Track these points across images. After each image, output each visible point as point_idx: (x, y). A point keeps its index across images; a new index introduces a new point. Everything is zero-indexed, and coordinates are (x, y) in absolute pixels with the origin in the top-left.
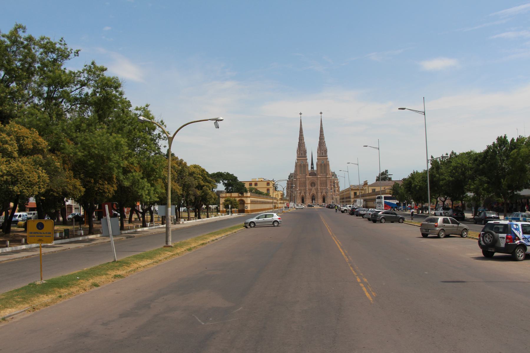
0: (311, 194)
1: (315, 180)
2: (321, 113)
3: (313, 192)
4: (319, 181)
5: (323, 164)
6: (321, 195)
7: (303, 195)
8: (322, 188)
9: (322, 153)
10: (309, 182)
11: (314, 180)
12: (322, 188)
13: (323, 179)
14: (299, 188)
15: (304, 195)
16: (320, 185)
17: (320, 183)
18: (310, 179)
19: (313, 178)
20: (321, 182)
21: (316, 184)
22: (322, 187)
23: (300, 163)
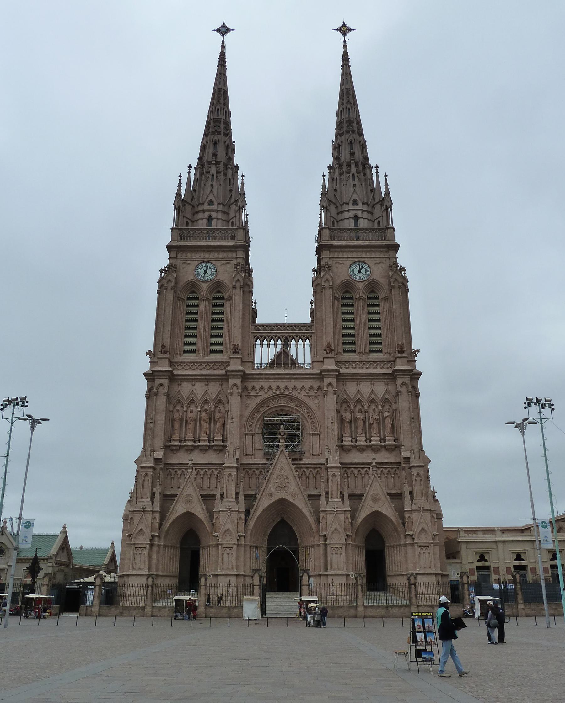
0: (263, 504)
1: (301, 396)
2: (344, 30)
3: (283, 487)
4: (330, 403)
5: (361, 286)
6: (353, 517)
7: (189, 515)
8: (355, 457)
9: (356, 218)
10: (256, 410)
11: (290, 398)
12: (355, 457)
13: (366, 388)
14: (159, 454)
15: (199, 510)
16: (341, 440)
17: (342, 420)
18: (258, 385)
19: (282, 384)
20: (348, 416)
21: (308, 429)
22: (362, 450)
23: (191, 277)
